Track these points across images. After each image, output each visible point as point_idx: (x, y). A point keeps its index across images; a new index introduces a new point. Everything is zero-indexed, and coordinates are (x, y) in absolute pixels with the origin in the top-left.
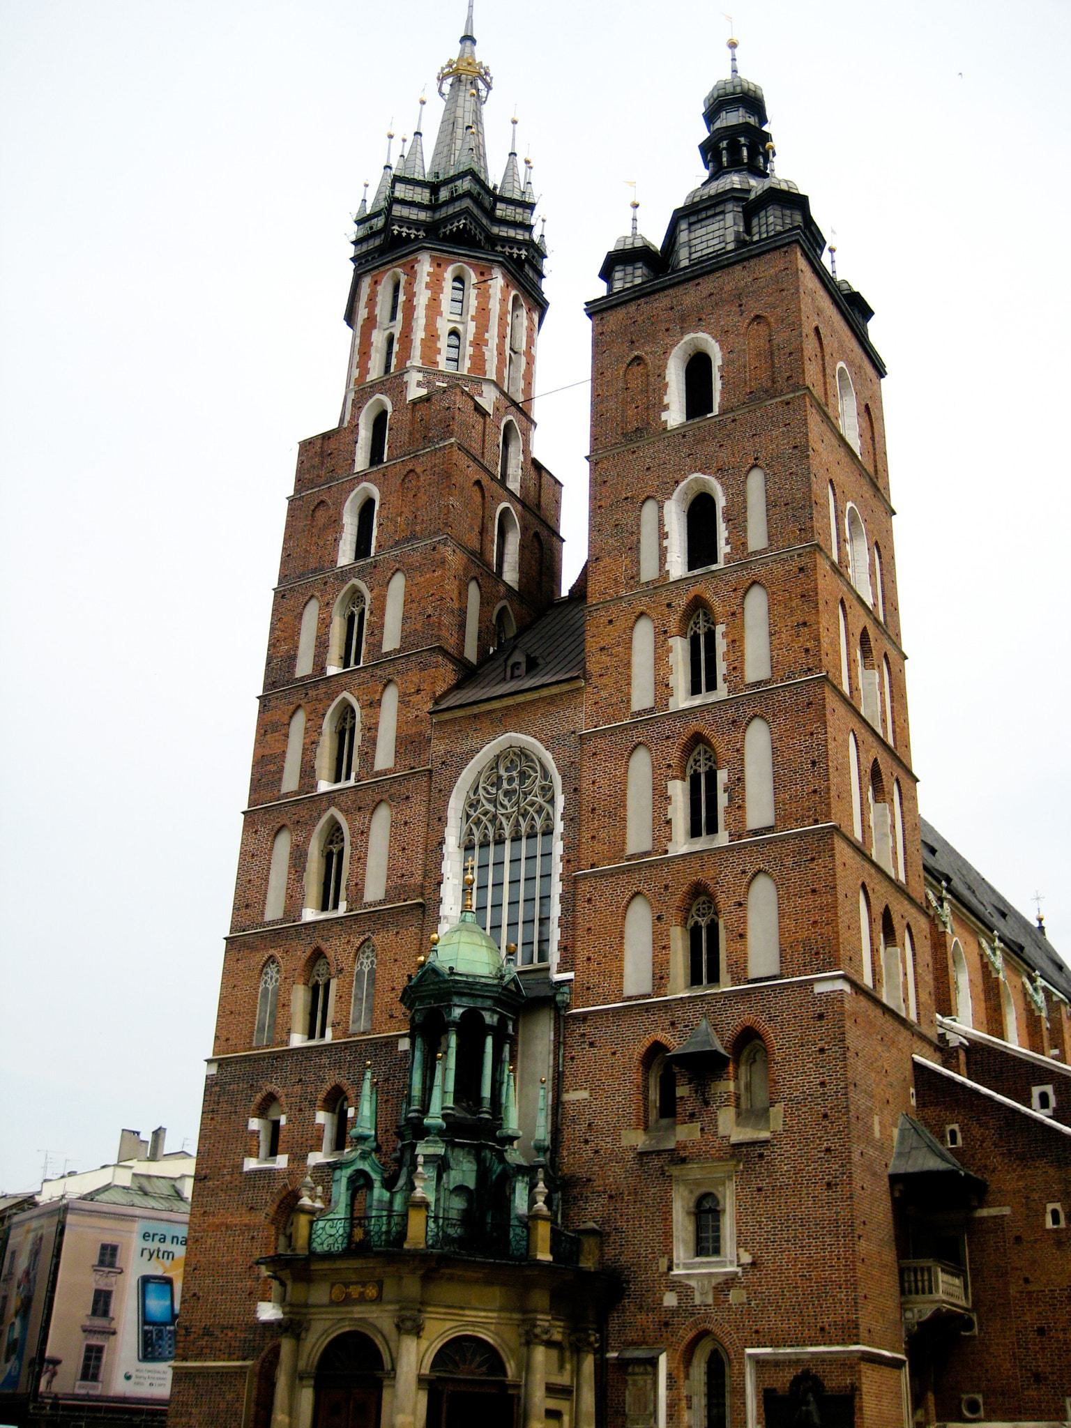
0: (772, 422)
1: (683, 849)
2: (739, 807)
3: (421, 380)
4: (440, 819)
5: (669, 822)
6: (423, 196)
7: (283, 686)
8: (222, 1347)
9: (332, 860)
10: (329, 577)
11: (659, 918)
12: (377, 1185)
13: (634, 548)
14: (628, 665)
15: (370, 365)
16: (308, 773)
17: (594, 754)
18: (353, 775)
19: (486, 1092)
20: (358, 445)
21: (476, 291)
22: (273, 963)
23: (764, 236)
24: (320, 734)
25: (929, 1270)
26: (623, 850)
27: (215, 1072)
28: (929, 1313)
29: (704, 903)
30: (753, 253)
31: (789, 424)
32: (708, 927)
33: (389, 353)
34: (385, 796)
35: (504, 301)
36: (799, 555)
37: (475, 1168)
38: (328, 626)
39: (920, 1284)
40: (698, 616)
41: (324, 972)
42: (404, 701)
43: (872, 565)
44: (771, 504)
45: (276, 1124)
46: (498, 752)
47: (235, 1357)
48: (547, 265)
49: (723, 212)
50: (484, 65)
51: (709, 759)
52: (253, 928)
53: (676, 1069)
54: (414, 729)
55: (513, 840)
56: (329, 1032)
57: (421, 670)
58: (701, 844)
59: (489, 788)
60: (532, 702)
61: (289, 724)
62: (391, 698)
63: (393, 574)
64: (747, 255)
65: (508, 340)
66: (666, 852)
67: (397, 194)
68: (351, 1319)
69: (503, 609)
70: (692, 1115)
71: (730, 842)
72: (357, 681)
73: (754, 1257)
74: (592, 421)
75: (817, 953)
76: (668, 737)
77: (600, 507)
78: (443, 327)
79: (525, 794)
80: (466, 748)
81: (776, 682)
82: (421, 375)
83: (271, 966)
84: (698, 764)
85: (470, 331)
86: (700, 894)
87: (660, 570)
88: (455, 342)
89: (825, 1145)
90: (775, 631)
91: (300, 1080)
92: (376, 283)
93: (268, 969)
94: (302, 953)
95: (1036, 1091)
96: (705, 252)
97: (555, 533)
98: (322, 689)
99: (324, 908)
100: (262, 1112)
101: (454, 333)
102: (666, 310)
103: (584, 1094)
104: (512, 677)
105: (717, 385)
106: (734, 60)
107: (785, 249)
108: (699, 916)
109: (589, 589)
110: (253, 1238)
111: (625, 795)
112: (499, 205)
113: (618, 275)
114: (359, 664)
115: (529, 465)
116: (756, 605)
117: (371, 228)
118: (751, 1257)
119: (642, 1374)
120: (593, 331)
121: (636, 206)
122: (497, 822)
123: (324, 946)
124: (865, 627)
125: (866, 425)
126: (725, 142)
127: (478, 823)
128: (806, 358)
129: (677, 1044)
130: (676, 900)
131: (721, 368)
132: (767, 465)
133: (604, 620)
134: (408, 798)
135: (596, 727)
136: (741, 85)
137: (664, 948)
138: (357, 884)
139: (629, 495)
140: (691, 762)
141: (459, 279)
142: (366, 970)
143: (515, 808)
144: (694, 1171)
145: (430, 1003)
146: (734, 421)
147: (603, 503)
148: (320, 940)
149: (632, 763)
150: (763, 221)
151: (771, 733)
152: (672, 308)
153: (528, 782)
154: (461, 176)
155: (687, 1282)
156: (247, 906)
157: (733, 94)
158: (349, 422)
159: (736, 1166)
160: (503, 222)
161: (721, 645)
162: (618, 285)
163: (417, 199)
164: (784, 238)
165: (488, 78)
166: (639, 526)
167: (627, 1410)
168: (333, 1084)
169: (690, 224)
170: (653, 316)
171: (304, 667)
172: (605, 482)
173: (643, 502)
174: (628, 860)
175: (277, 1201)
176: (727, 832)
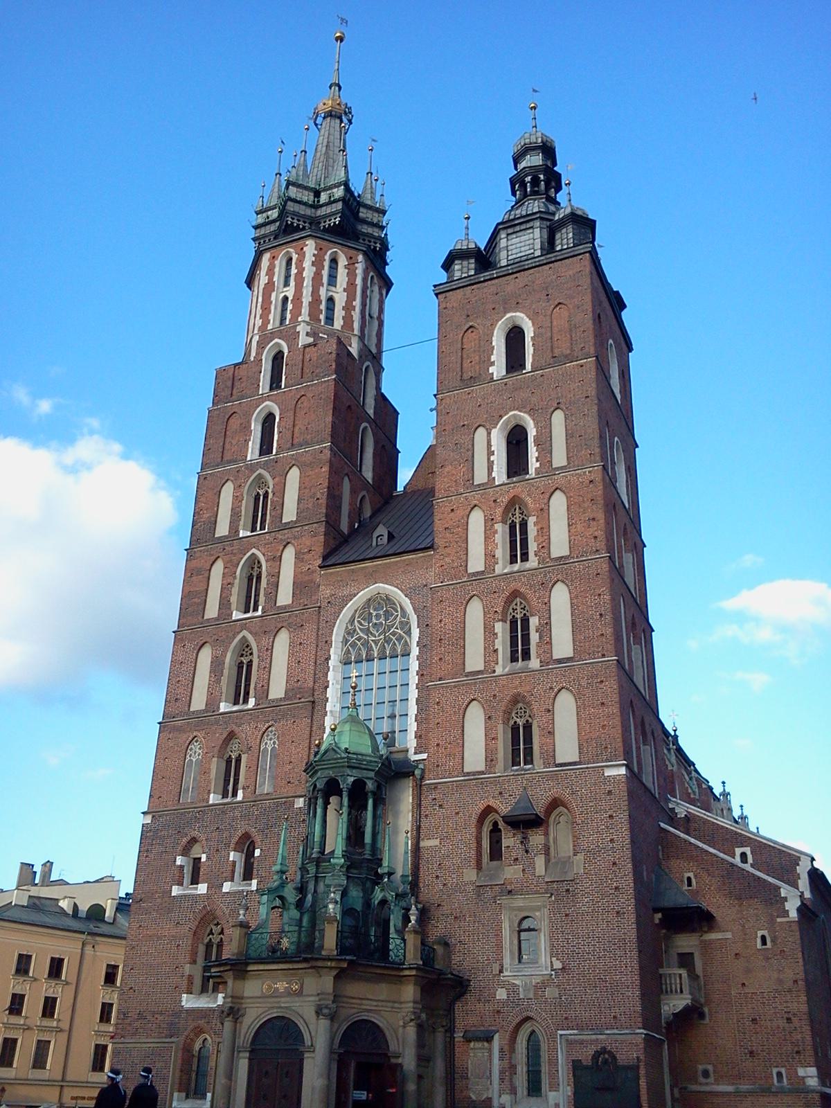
0: (570, 379)
4: (326, 642)
5: (496, 651)
6: (308, 197)
7: (206, 542)
8: (153, 1028)
9: (243, 671)
10: (241, 467)
15: (271, 317)
16: (224, 604)
17: (441, 601)
18: (260, 608)
19: (368, 839)
20: (262, 374)
22: (196, 741)
23: (565, 247)
24: (235, 578)
25: (680, 975)
27: (150, 822)
28: (681, 1007)
29: (521, 708)
30: (558, 258)
33: (284, 309)
34: (284, 624)
35: (364, 280)
37: (361, 895)
38: (241, 501)
39: (673, 986)
40: (515, 510)
42: (299, 557)
44: (569, 436)
45: (197, 861)
47: (163, 1035)
48: (389, 255)
49: (532, 227)
50: (349, 106)
51: (524, 609)
53: (501, 825)
54: (307, 578)
57: (312, 536)
59: (362, 622)
61: (210, 570)
62: (289, 555)
63: (290, 468)
64: (553, 259)
66: (494, 671)
67: (293, 196)
69: (364, 496)
71: (541, 666)
73: (563, 964)
76: (495, 592)
78: (323, 293)
79: (390, 627)
81: (573, 558)
82: (309, 327)
85: (340, 299)
87: (488, 477)
89: (615, 885)
91: (218, 828)
92: (274, 257)
93: (193, 746)
94: (220, 735)
95: (738, 851)
99: (236, 703)
100: (185, 852)
103: (436, 842)
107: (581, 257)
108: (517, 717)
110: (179, 945)
112: (361, 210)
114: (265, 529)
116: (559, 503)
117: (268, 217)
118: (561, 964)
119: (480, 1048)
121: (468, 218)
123: (236, 729)
126: (530, 177)
130: (502, 706)
135: (442, 582)
138: (263, 686)
139: (466, 423)
143: (382, 637)
144: (519, 902)
145: (329, 774)
146: (542, 376)
147: (447, 428)
148: (234, 727)
154: (337, 186)
155: (514, 981)
158: (255, 357)
159: (550, 897)
160: (364, 221)
161: (532, 531)
162: (457, 275)
163: (305, 199)
166: (473, 445)
167: (469, 1075)
169: (508, 235)
171: (222, 529)
174: (466, 676)
175: (199, 917)
176: (539, 660)
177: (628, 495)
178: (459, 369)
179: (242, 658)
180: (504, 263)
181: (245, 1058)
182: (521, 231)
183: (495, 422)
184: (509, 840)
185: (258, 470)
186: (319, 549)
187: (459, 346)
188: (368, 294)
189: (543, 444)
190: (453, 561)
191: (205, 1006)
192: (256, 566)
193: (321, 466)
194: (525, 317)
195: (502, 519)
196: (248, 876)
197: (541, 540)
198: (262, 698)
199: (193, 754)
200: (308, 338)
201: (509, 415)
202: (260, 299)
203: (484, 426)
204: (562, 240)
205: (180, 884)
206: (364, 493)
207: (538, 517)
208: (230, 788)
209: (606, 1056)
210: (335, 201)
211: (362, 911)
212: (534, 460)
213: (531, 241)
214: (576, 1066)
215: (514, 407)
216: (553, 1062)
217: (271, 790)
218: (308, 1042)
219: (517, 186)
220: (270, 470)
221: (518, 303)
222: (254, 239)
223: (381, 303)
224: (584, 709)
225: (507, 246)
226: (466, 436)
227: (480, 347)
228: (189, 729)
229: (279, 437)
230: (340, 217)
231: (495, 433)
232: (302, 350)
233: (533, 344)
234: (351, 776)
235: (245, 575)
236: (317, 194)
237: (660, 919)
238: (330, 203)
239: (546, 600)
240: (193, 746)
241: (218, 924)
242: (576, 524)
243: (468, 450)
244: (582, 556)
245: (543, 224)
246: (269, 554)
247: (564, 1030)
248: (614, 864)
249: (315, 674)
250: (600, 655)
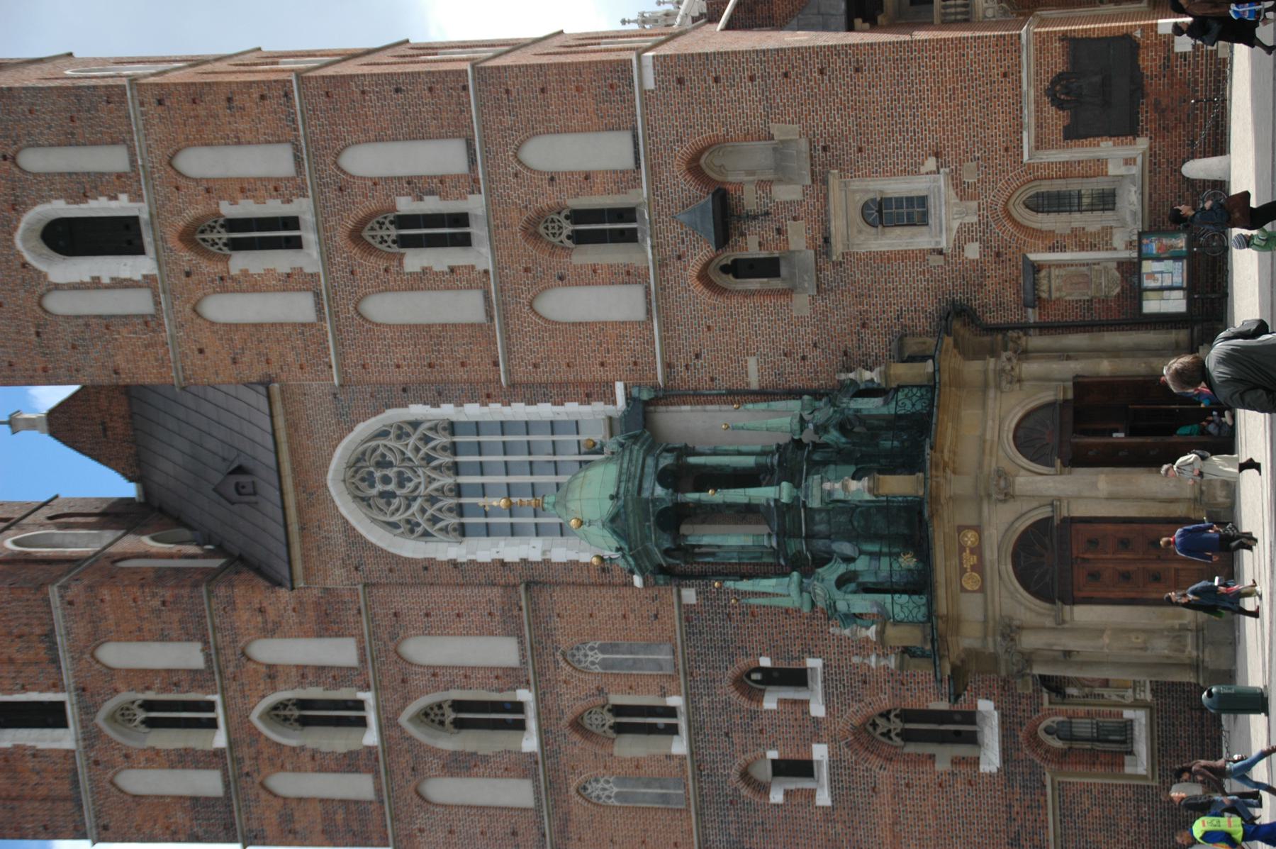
1: (485, 250)
2: (441, 182)
5: (452, 270)
7: (232, 812)
10: (88, 758)
11: (561, 278)
12: (852, 567)
13: (108, 322)
14: (258, 326)
16: (351, 762)
17: (364, 366)
18: (361, 695)
19: (750, 461)
22: (585, 789)
24: (303, 748)
26: (480, 325)
32: (575, 222)
37: (832, 467)
40: (204, 240)
41: (599, 717)
42: (272, 630)
44: (69, 139)
46: (349, 498)
52: (542, 822)
54: (310, 613)
55: (457, 473)
56: (675, 701)
58: (478, 230)
59: (393, 507)
60: (293, 451)
61: (285, 799)
62: (268, 651)
63: (98, 662)
66: (486, 272)
68: (999, 562)
70: (779, 231)
71: (480, 193)
72: (239, 700)
75: (611, 86)
76: (352, 273)
77: (45, 370)
79: (405, 459)
80: (339, 539)
81: (297, 137)
83: (589, 791)
84: (386, 238)
86: (535, 228)
87: (140, 287)
91: (727, 734)
94: (575, 746)
98: (245, 752)
99: (520, 726)
100: (763, 789)
103: (752, 364)
104: (255, 493)
108: (560, 234)
110: (907, 785)
111: (416, 326)
118: (930, 159)
119: (1050, 281)
122: (434, 494)
123: (569, 716)
127: (434, 520)
129: (702, 252)
132: (15, 144)
134: (395, 614)
135: (331, 367)
137: (595, 271)
138: (497, 677)
139: (33, 330)
140: (383, 247)
142: (601, 656)
143: (420, 471)
144: (837, 226)
147: (39, 366)
149: (378, 319)
151: (358, 143)
153: (390, 457)
155: (954, 232)
156: (514, 834)
161: (246, 208)
167: (1087, 298)
168: (732, 689)
171: (208, 783)
172: (11, 365)
173: (46, 311)
174: (492, 318)
175: (864, 754)
179: (447, 721)
181: (1072, 612)
183: (35, 276)
184: (751, 247)
185: (96, 726)
186: (260, 594)
189: (84, 188)
190: (293, 348)
191: (996, 730)
192: (282, 713)
195: (221, 260)
196: (799, 678)
197: (263, 192)
198: (517, 677)
199: (607, 793)
203: (42, 296)
205: (811, 794)
207: (220, 198)
208: (661, 721)
209: (1058, 88)
211: (856, 464)
212: (113, 204)
214: (1073, 133)
215: (8, 240)
216: (1067, 170)
217: (667, 647)
218: (1045, 513)
220: (98, 699)
224: (550, 121)
226: (60, 329)
228: (564, 805)
229: (33, 690)
234: (653, 490)
235: (297, 732)
237: (864, 22)
239: (370, 183)
240: (593, 795)
241: (874, 725)
242: (237, 130)
243: (87, 325)
244: (294, 121)
246: (262, 687)
247: (1022, 152)
248: (786, 75)
249: (480, 584)
250: (463, 94)
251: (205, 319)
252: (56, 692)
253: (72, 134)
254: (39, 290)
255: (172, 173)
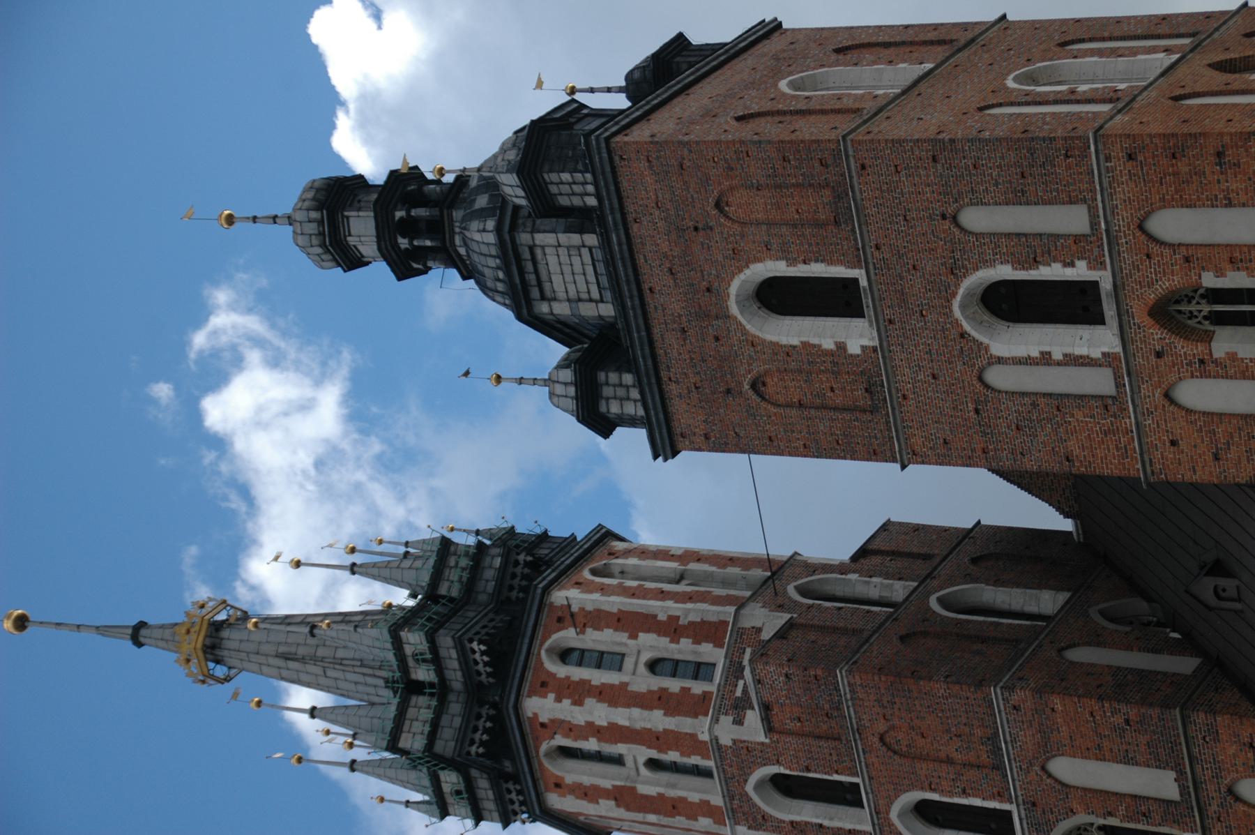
3: (730, 718)
6: (422, 708)
13: (1060, 401)
15: (694, 797)
20: (826, 823)
21: (589, 630)
23: (590, 188)
30: (616, 206)
31: (896, 166)
33: (675, 768)
35: (603, 589)
36: (1108, 159)
40: (1180, 312)
43: (1100, 53)
44: (1019, 197)
49: (532, 249)
57: (1217, 739)
63: (1050, 776)
64: (618, 216)
65: (667, 587)
74: (845, 458)
77: (984, 451)
78: (645, 682)
82: (722, 718)
85: (651, 644)
87: (1100, 366)
88: (668, 667)
90: (1225, 198)
96: (592, 278)
97: (967, 534)
101: (654, 666)
102: (685, 340)
105: (818, 270)
106: (255, 219)
107: (617, 158)
109: (1116, 472)
112: (443, 590)
113: (614, 408)
115: (858, 565)
117: (458, 793)
120: (700, 450)
121: (499, 379)
124: (1209, 65)
125: (867, 55)
128: (793, 137)
131: (792, 262)
132: (957, 201)
133: (1170, 453)
136: (308, 210)
139: (971, 407)
141: (565, 655)
147: (979, 447)
150: (565, 189)
152: (684, 331)
154: (398, 644)
157: (320, 222)
160: (470, 587)
163: (427, 715)
164: (601, 158)
165: (211, 604)
166: (1023, 394)
170: (692, 359)
172: (945, 442)
173: (987, 386)
177: (1134, 52)
178: (848, 416)
180: (608, 310)
182: (536, 272)
187: (794, 412)
188: (634, 584)
193: (1048, 710)
194: (742, 276)
200: (746, 722)
201: (961, 318)
202: (652, 818)
204: (574, 194)
206: (1094, 613)
207: (1203, 269)
210: (434, 648)
213: (563, 252)
219: (415, 266)
221: (708, 290)
222: (506, 824)
223: (644, 552)
225: (569, 300)
227: (800, 371)
229: (975, 796)
230: (471, 641)
231: (999, 348)
232: (776, 737)
233: (805, 263)
236: (415, 688)
238: (436, 660)
243: (1034, 405)
245: (524, 224)
251: (1180, 407)
252: (1002, 802)
253: (1023, 192)
254: (979, 363)
255: (1143, 238)
